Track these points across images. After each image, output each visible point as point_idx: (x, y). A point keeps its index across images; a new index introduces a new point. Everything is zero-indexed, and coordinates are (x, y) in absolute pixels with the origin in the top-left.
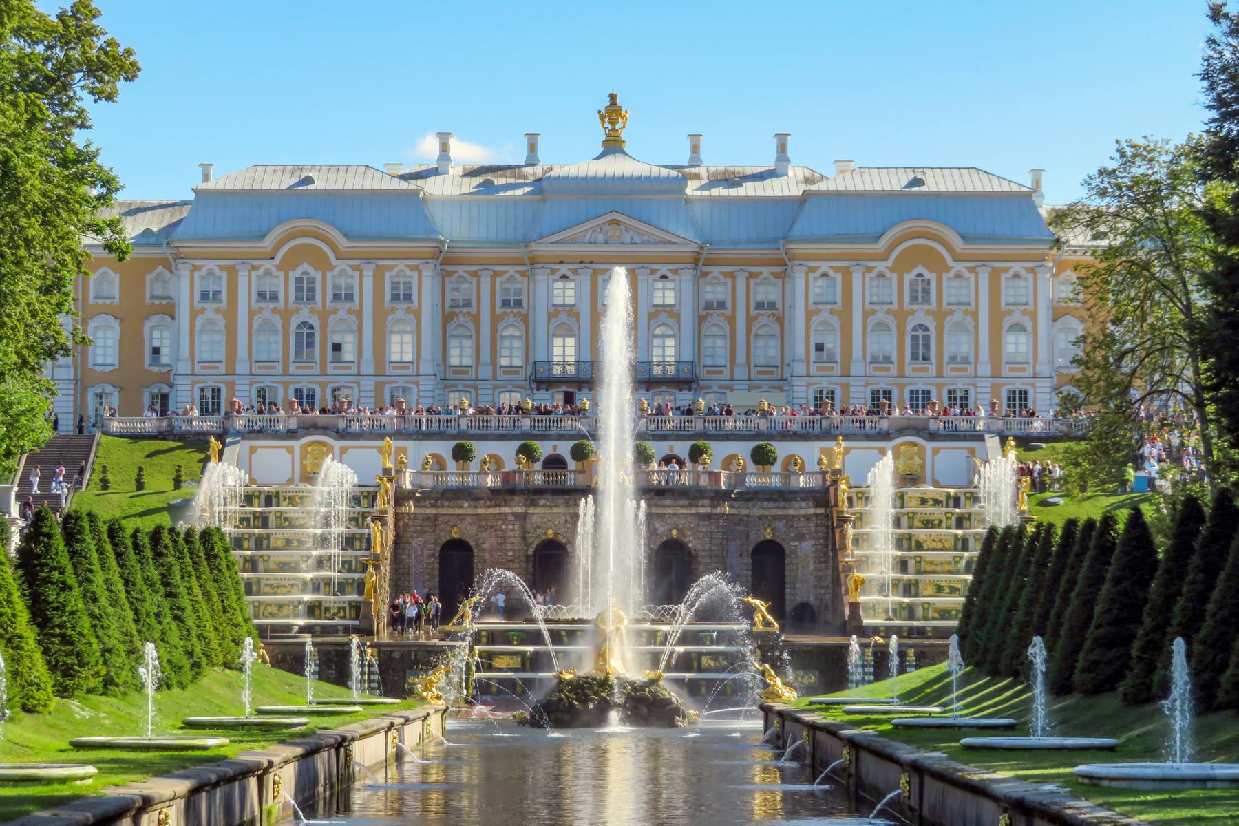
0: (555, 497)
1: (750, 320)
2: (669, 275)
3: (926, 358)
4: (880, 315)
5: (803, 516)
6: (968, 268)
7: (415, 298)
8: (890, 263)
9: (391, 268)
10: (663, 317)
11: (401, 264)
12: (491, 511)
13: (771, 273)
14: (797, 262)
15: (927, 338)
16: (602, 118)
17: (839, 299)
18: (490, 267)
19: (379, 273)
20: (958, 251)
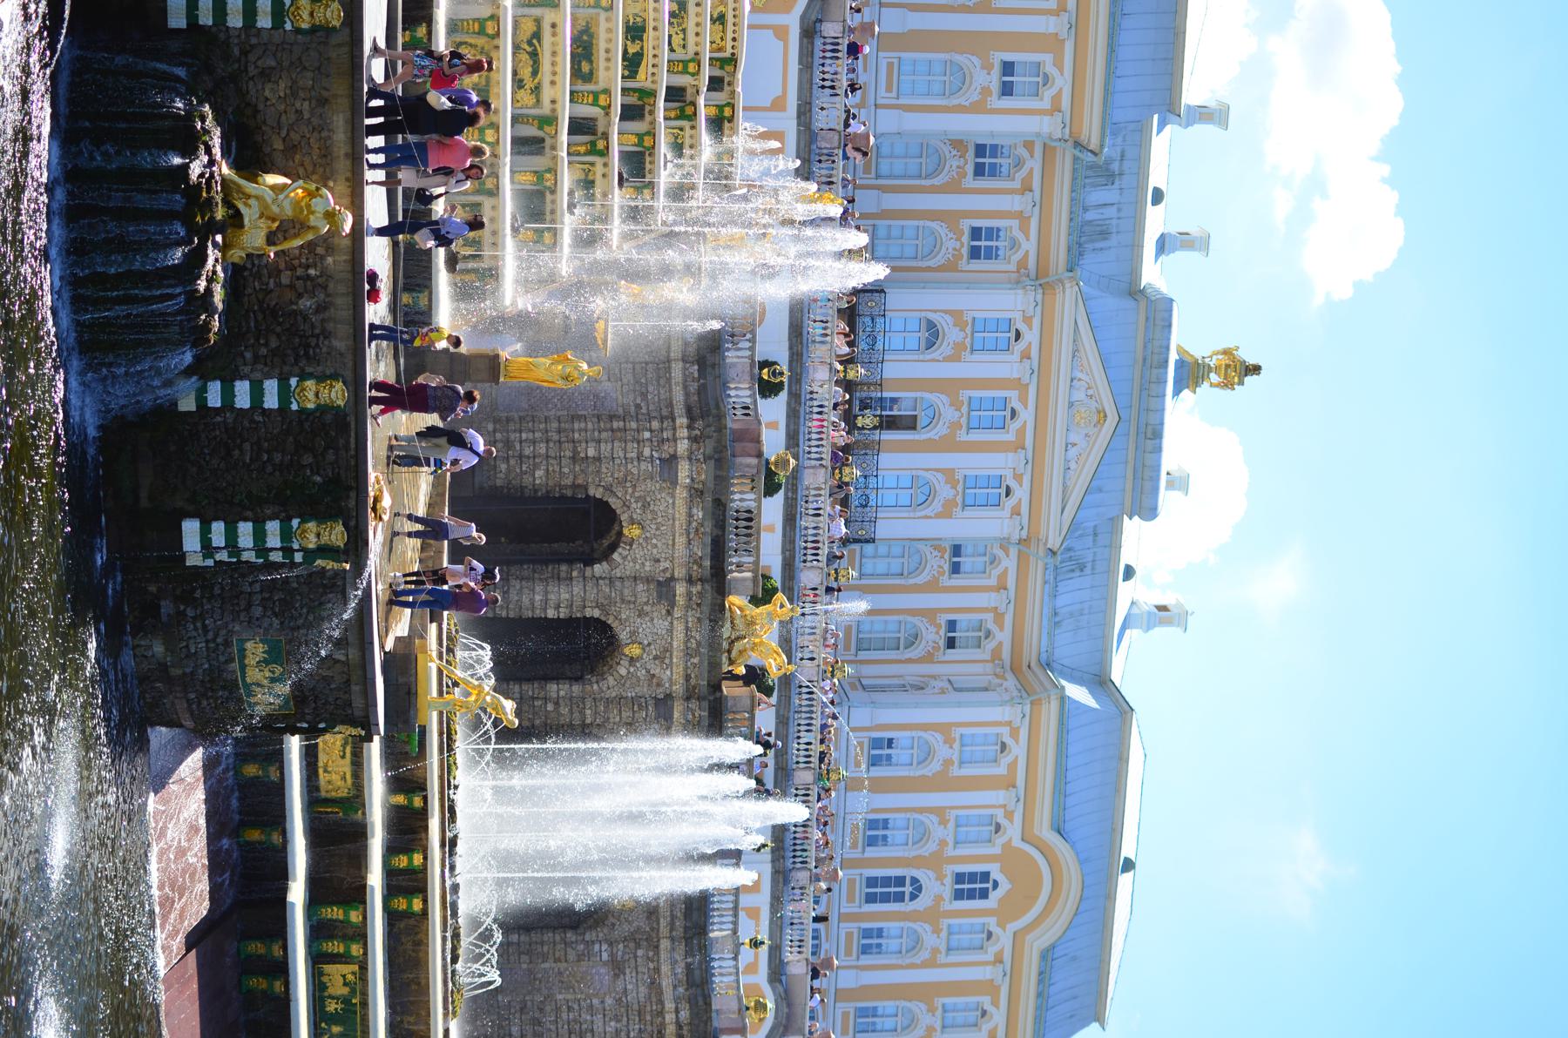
0: (708, 540)
1: (930, 614)
2: (1009, 503)
3: (871, 898)
4: (938, 832)
5: (657, 970)
6: (1001, 952)
7: (1007, 102)
8: (1017, 843)
9: (1059, 65)
10: (945, 492)
11: (1062, 83)
12: (678, 396)
13: (1001, 643)
14: (1027, 708)
15: (899, 898)
16: (1226, 352)
17: (968, 771)
18: (1037, 209)
19: (1051, 43)
20: (1029, 937)
